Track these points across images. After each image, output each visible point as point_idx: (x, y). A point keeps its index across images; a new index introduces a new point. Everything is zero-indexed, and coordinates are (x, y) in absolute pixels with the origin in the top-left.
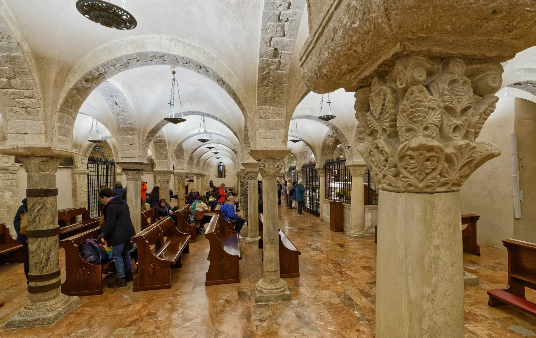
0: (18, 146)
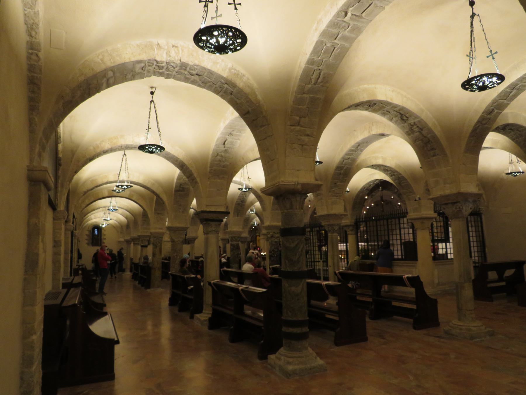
0: (299, 182)
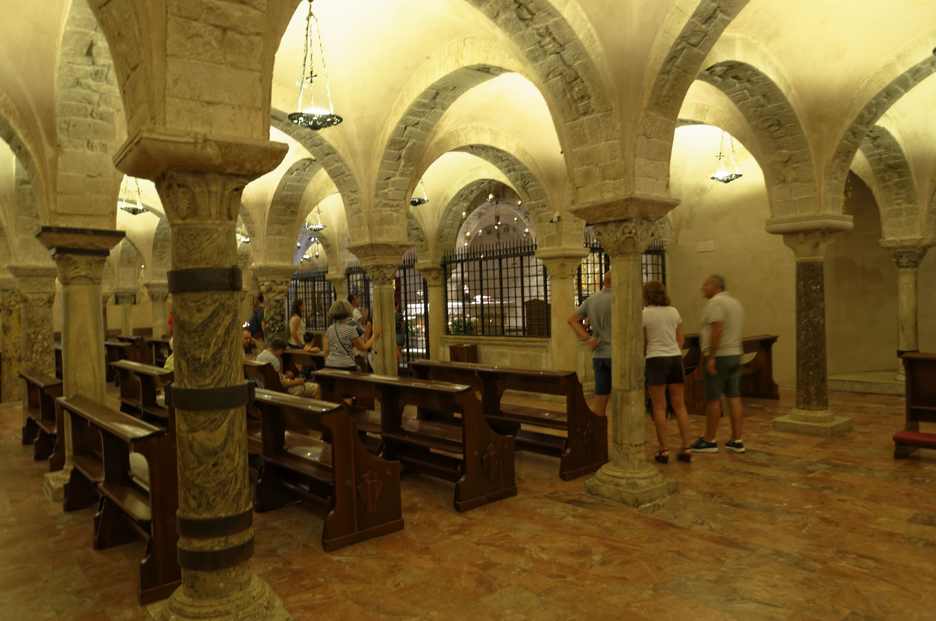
0: (210, 137)
